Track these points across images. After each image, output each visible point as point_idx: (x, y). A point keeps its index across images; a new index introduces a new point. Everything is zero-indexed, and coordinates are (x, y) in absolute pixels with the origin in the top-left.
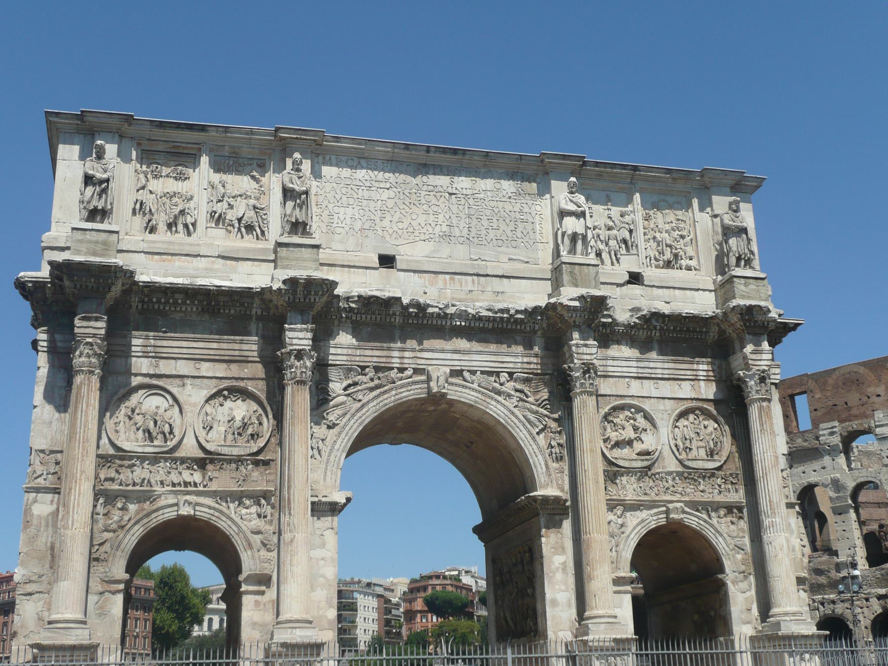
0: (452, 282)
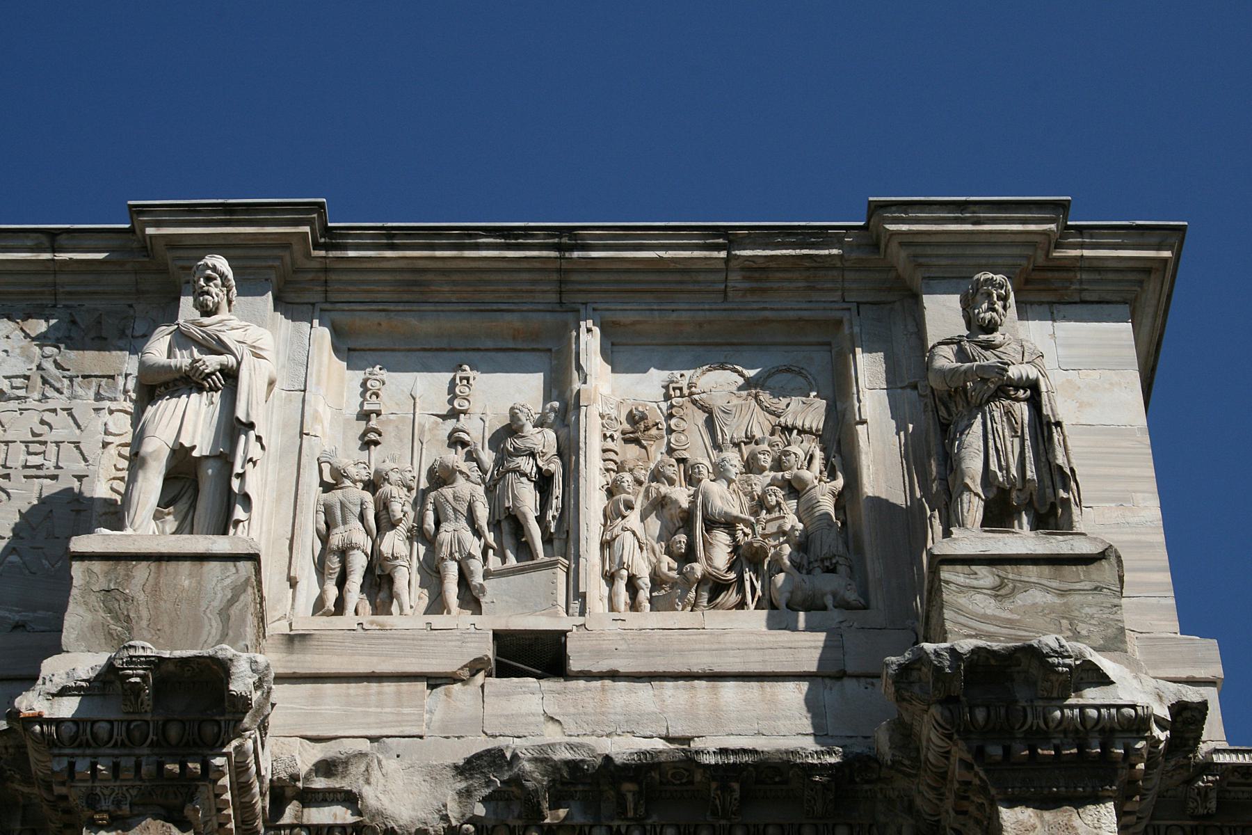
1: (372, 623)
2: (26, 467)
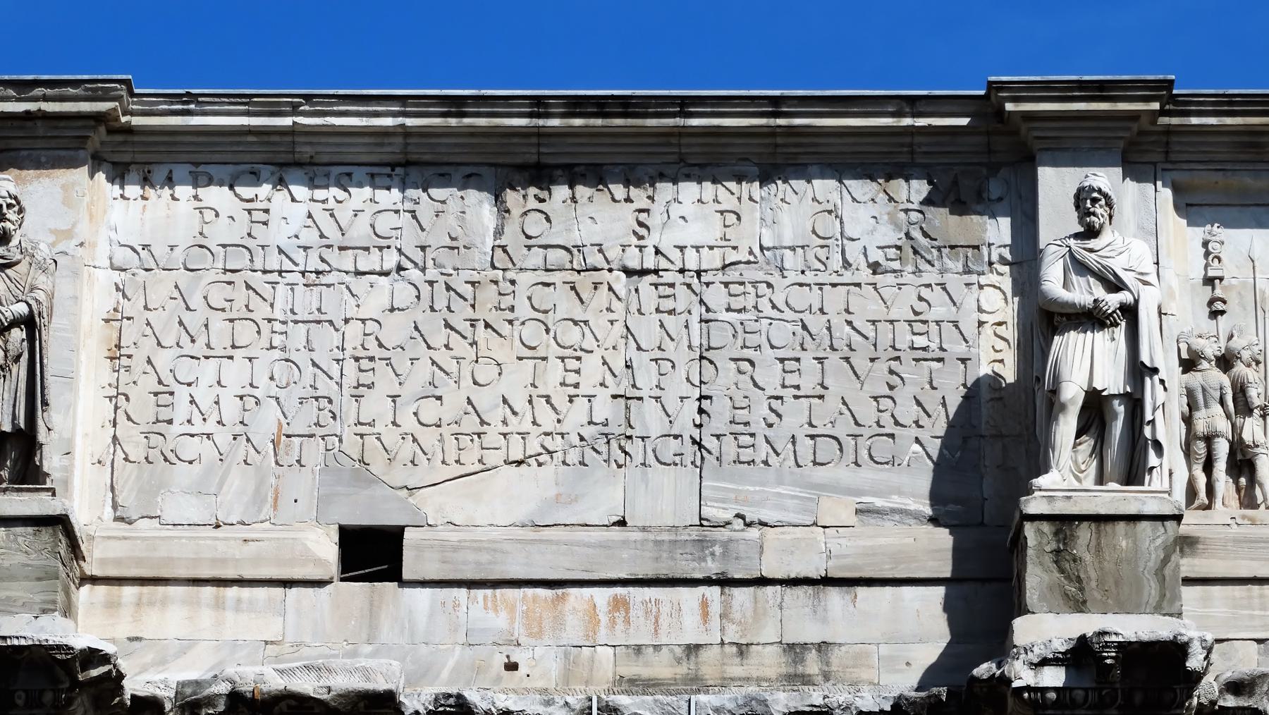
0: (620, 616)
1: (1244, 517)
2: (913, 348)
